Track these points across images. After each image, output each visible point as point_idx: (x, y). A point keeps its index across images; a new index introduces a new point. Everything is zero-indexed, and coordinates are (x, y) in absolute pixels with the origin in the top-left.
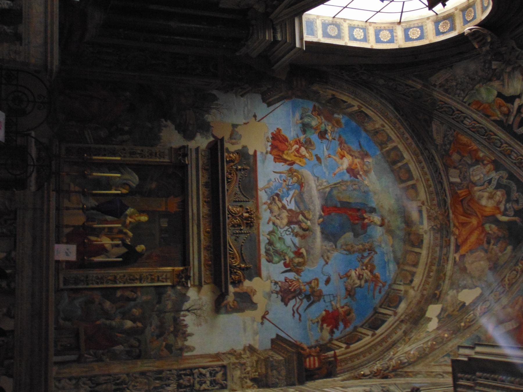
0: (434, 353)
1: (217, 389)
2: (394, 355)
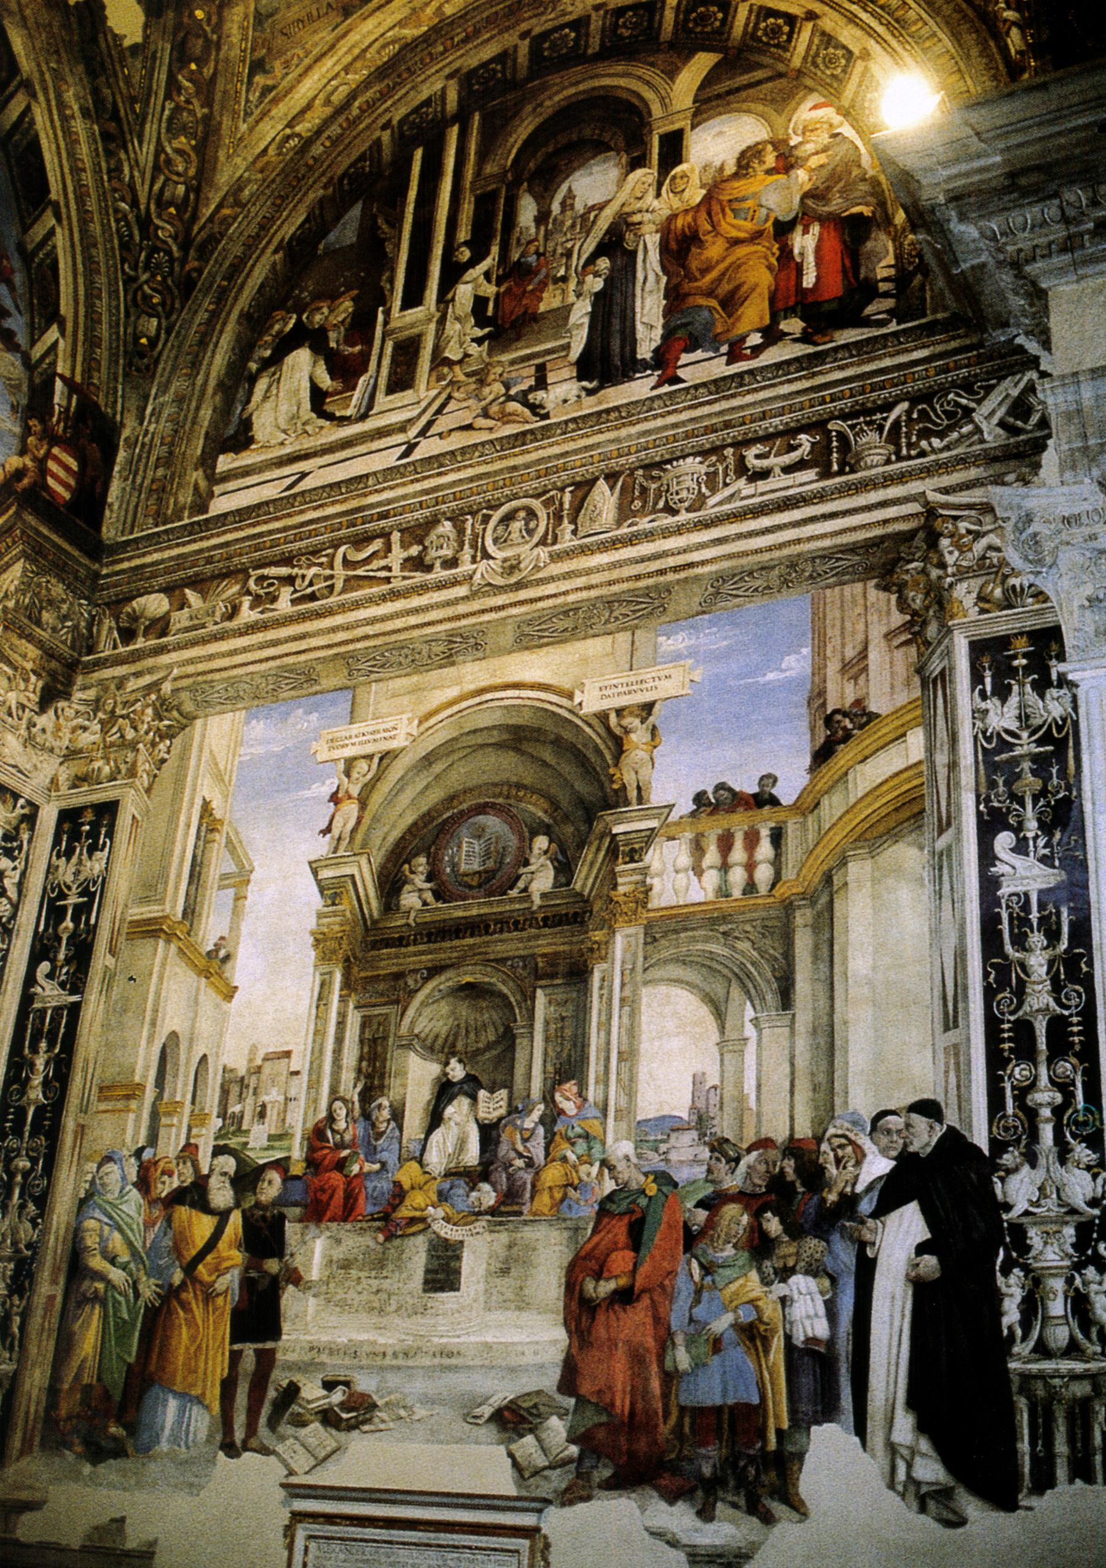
0: (218, 96)
1: (30, 841)
2: (135, 203)
